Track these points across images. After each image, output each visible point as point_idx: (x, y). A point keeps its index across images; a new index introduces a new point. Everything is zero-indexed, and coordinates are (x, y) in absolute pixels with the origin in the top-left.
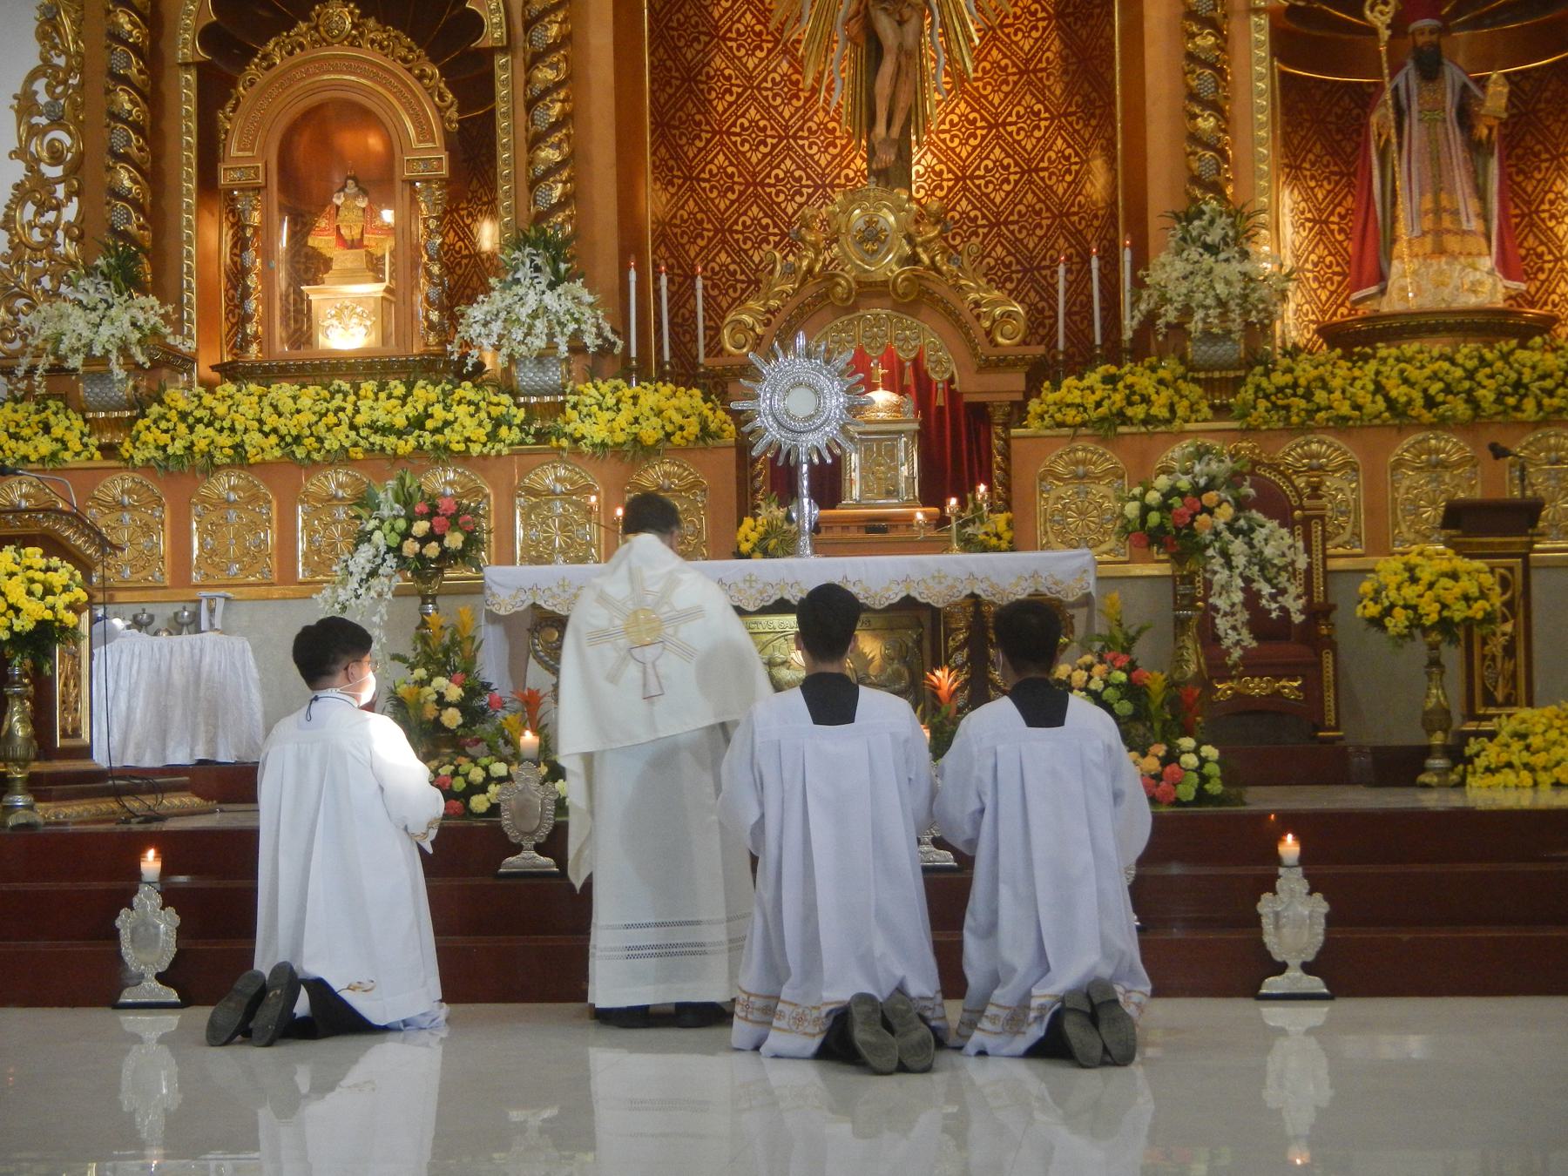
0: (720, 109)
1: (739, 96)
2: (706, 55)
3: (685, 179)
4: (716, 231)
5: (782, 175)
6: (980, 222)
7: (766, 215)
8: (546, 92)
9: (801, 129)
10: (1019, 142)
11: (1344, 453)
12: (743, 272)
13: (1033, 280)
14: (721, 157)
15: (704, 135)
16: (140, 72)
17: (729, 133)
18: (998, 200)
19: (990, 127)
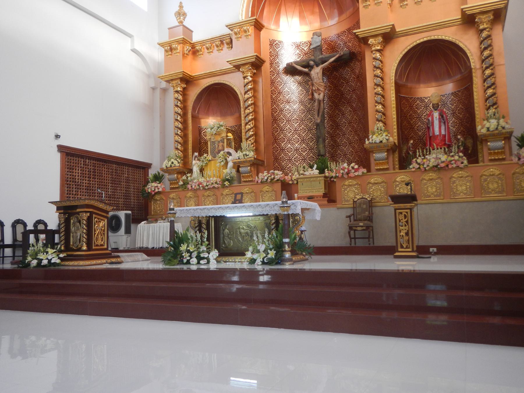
0: (288, 116)
1: (292, 113)
2: (285, 106)
3: (281, 130)
4: (288, 140)
5: (301, 128)
6: (341, 135)
7: (298, 137)
8: (248, 114)
9: (305, 119)
10: (348, 117)
11: (409, 178)
12: (294, 148)
13: (351, 146)
14: (289, 126)
15: (285, 122)
16: (180, 118)
17: (290, 121)
18: (344, 130)
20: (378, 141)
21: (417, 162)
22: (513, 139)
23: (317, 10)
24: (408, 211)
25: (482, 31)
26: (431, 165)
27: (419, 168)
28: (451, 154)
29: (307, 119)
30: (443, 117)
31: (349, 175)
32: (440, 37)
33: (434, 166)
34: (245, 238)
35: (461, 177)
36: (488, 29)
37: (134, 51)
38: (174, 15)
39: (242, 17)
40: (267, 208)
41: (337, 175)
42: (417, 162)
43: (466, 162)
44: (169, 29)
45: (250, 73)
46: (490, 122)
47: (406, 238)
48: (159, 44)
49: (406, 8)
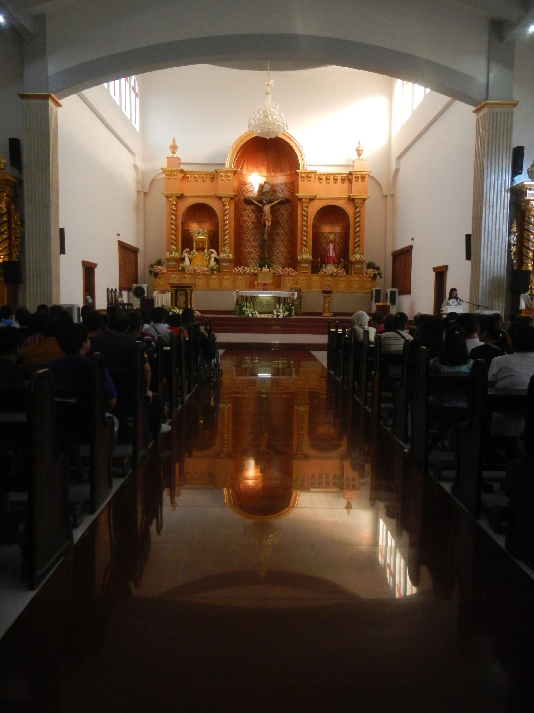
8: (227, 229)
19: (278, 235)
20: (305, 258)
21: (323, 271)
22: (364, 264)
23: (266, 164)
24: (329, 297)
25: (357, 207)
26: (330, 273)
27: (324, 274)
28: (339, 268)
29: (256, 234)
30: (335, 248)
31: (289, 274)
32: (337, 205)
33: (331, 274)
34: (265, 306)
35: (342, 280)
36: (360, 208)
37: (135, 166)
38: (169, 146)
39: (227, 167)
40: (282, 294)
41: (283, 274)
42: (323, 271)
43: (345, 273)
44: (167, 157)
45: (229, 203)
46: (356, 255)
47: (328, 309)
48: (162, 169)
49: (321, 183)
